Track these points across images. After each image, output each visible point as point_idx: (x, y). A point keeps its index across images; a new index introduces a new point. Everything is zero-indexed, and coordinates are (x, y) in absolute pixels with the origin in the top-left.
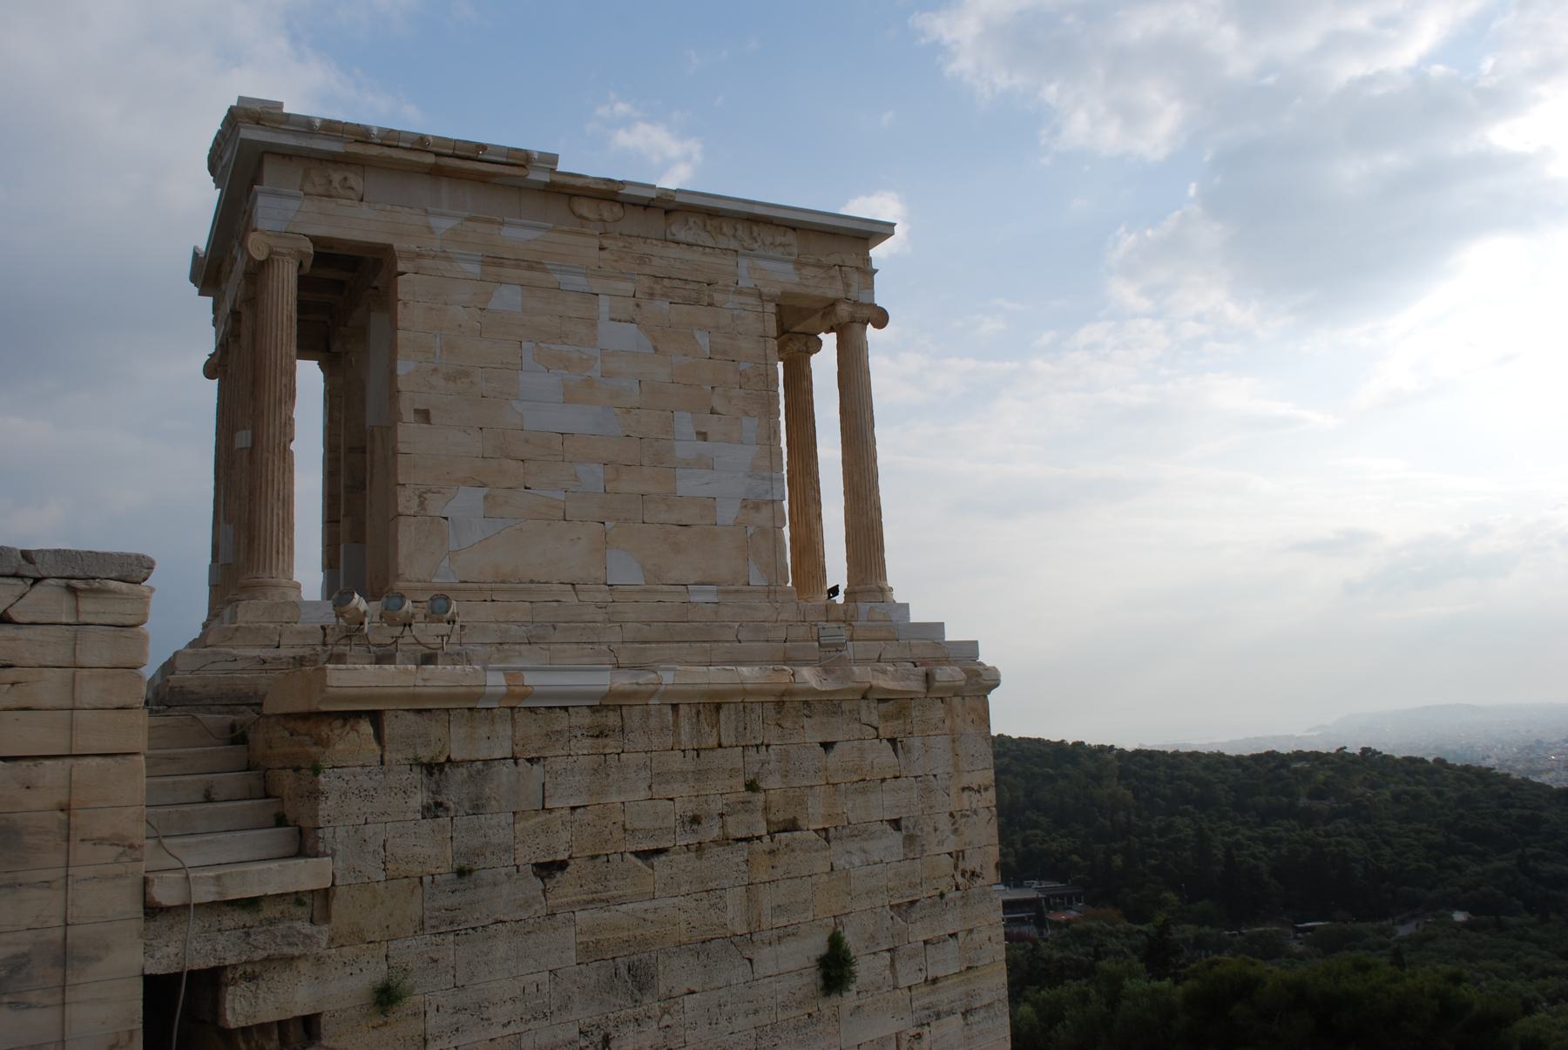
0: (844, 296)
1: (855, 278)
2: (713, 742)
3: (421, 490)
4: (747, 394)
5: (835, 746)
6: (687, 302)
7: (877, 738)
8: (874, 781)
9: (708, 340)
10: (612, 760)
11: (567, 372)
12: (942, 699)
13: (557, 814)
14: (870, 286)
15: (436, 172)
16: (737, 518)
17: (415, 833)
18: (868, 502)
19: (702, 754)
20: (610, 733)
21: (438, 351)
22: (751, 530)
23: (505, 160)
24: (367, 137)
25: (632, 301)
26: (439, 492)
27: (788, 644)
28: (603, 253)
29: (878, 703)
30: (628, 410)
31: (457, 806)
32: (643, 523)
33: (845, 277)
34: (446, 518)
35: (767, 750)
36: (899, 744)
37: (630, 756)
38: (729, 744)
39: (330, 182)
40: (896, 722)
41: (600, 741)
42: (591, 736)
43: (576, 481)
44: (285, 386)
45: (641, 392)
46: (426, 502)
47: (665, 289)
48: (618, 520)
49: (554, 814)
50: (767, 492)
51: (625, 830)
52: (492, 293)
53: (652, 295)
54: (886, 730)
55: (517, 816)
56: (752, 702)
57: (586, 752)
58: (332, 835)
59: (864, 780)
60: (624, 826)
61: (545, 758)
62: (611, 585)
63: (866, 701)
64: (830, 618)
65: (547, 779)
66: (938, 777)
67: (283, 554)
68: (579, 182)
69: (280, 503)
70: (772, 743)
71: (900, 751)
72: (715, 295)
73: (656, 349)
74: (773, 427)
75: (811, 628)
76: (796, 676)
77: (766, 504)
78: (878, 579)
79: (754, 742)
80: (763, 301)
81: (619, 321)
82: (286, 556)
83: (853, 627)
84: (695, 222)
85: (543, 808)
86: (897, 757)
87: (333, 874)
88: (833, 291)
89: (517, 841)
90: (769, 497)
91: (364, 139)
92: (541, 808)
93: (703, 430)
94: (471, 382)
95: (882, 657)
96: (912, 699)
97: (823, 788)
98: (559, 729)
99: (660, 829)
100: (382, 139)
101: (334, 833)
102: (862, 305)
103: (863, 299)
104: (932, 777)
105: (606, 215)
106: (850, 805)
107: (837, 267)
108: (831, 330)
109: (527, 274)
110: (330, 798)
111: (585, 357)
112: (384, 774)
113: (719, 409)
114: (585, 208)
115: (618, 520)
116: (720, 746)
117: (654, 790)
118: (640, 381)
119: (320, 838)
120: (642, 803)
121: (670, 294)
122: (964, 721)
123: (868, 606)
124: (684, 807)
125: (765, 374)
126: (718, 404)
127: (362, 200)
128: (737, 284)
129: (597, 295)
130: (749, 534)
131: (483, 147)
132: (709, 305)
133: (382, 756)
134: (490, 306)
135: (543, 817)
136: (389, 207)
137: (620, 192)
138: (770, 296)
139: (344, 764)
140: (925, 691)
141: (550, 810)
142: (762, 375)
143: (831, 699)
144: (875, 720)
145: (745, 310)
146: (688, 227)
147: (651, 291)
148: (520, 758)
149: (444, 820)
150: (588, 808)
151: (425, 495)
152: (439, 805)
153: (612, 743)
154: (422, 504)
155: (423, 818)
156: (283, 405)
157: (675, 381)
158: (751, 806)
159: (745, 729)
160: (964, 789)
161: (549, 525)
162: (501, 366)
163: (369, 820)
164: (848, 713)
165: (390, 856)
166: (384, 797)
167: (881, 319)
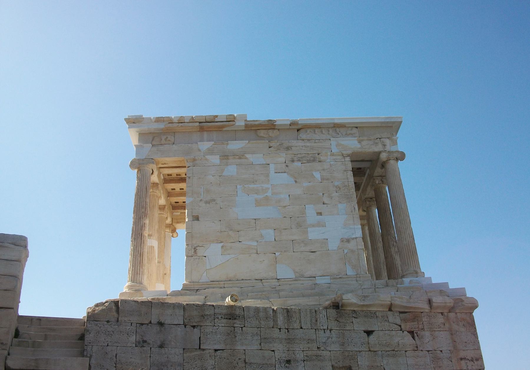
0: (383, 150)
1: (387, 142)
2: (296, 325)
3: (196, 246)
4: (340, 194)
5: (374, 333)
6: (309, 161)
7: (401, 330)
8: (400, 351)
9: (320, 175)
10: (238, 330)
11: (257, 195)
13: (207, 352)
14: (395, 143)
15: (202, 129)
16: (338, 247)
17: (132, 352)
19: (291, 331)
20: (237, 318)
21: (202, 193)
22: (346, 251)
23: (225, 120)
24: (172, 121)
25: (284, 165)
26: (202, 246)
28: (270, 148)
30: (285, 207)
31: (154, 343)
32: (294, 252)
34: (205, 257)
35: (330, 332)
36: (415, 334)
37: (249, 329)
38: (307, 328)
39: (162, 139)
41: (231, 320)
42: (226, 318)
43: (262, 237)
44: (143, 212)
45: (290, 199)
46: (197, 251)
47: (299, 158)
48: (282, 251)
49: (205, 352)
50: (353, 234)
51: (246, 363)
52: (224, 169)
53: (293, 161)
54: (409, 326)
55: (185, 351)
57: (223, 325)
58: (91, 349)
59: (394, 350)
60: (245, 361)
61: (201, 326)
62: (279, 279)
63: (392, 312)
65: (202, 336)
66: (443, 352)
67: (139, 274)
68: (257, 123)
69: (139, 255)
70: (333, 328)
71: (416, 338)
72: (321, 157)
73: (296, 182)
74: (354, 207)
78: (414, 268)
79: (322, 328)
80: (344, 157)
81: (279, 173)
82: (141, 275)
84: (310, 131)
85: (200, 348)
86: (414, 340)
87: (89, 364)
88: (376, 149)
89: (185, 361)
90: (354, 236)
91: (172, 122)
92: (198, 348)
93: (320, 211)
94: (216, 203)
96: (422, 313)
97: (367, 353)
98: (209, 314)
99: (267, 364)
100: (178, 121)
101: (92, 348)
103: (393, 149)
104: (439, 352)
105: (271, 134)
106: (385, 362)
109: (239, 160)
110: (91, 333)
111: (264, 188)
112: (118, 325)
113: (326, 202)
114: (262, 133)
115: (282, 251)
116: (301, 328)
117: (262, 346)
118: (289, 195)
119: (85, 349)
120: (256, 351)
121: (301, 160)
124: (280, 355)
125: (348, 185)
126: (326, 200)
127: (174, 144)
129: (269, 164)
130: (345, 253)
131: (217, 116)
132: (320, 162)
133: (118, 318)
134: (224, 174)
135: (198, 352)
136: (183, 145)
137: (274, 124)
138: (347, 154)
139: (99, 320)
141: (204, 350)
142: (346, 186)
143: (370, 310)
144: (398, 321)
146: (307, 133)
147: (292, 160)
148: (187, 325)
149: (147, 348)
150: (224, 350)
151: (196, 248)
152: (145, 342)
153: (238, 322)
154: (195, 252)
155: (136, 346)
156: (142, 219)
157: (305, 193)
158: (321, 358)
159: (316, 321)
160: (461, 359)
161: (250, 256)
162: (228, 196)
163: (109, 344)
164: (380, 317)
165: (119, 361)
166: (117, 335)
167: (401, 156)
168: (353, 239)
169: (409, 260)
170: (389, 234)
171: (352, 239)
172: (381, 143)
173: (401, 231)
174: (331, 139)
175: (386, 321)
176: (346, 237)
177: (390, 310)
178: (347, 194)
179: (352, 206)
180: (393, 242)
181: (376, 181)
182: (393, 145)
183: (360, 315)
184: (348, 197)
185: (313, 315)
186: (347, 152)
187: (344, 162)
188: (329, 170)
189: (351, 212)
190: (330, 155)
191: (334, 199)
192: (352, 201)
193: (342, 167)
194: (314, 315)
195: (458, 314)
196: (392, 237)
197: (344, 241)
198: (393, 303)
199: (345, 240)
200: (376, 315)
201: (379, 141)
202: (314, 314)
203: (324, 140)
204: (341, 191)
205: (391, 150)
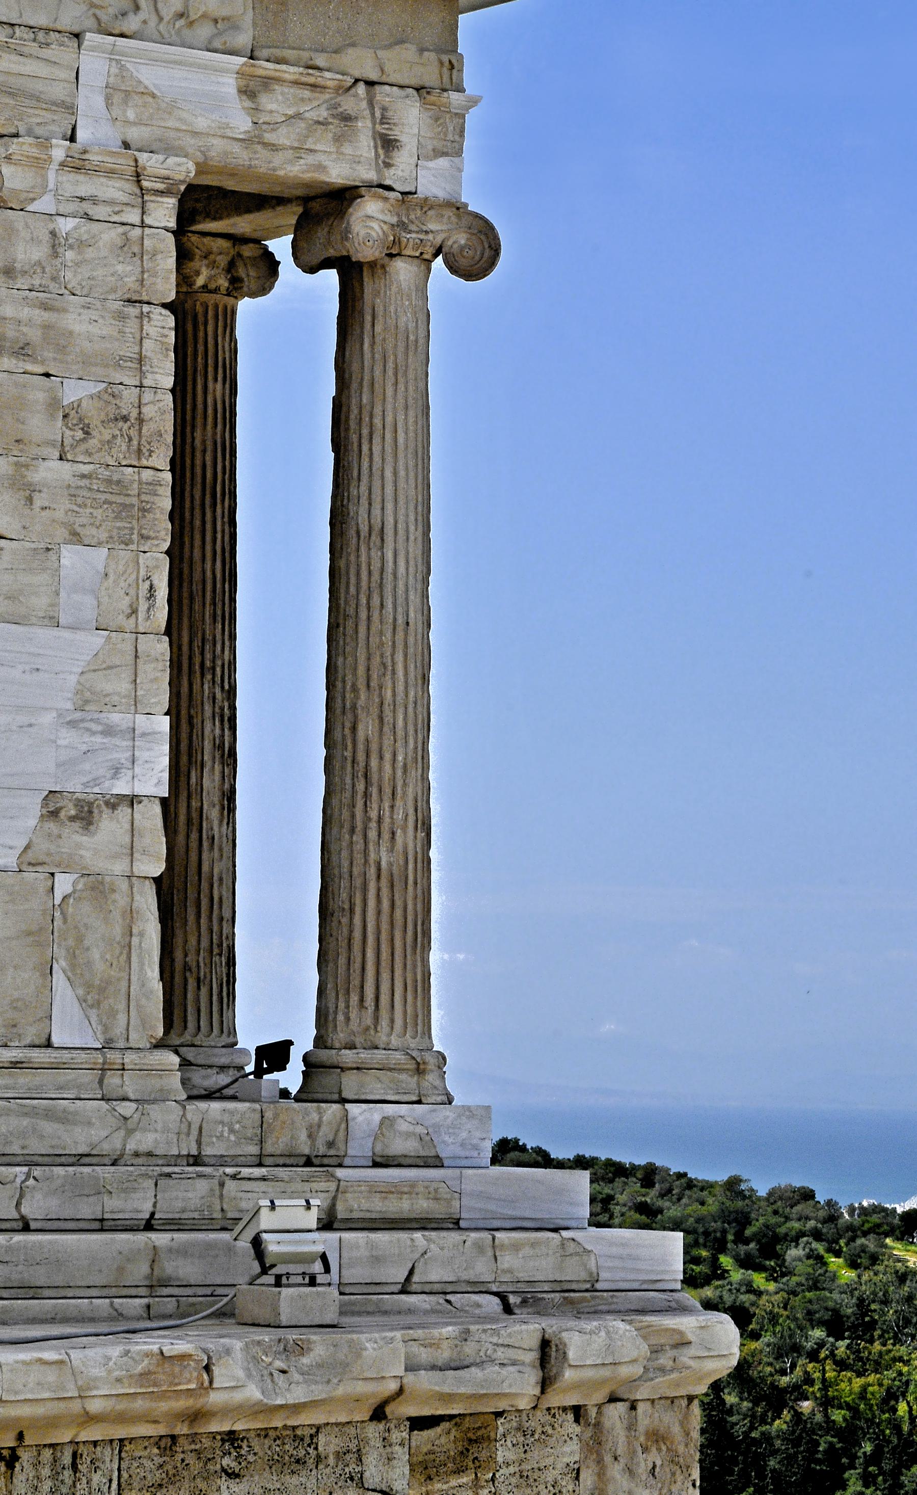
0: (371, 175)
4: (83, 476)
12: (578, 1412)
16: (27, 847)
18: (399, 803)
22: (64, 884)
27: (160, 1239)
29: (412, 1429)
33: (384, 120)
40: (454, 1482)
50: (116, 771)
56: (95, 1443)
63: (381, 1426)
64: (269, 1148)
75: (222, 1185)
76: (216, 1370)
77: (113, 806)
83: (339, 1181)
90: (121, 787)
95: (416, 1278)
96: (499, 1414)
102: (427, 205)
107: (361, 89)
108: (327, 264)
122: (630, 1471)
123: (377, 1113)
125: (134, 414)
128: (72, 139)
130: (57, 901)
140: (537, 1391)
142: (125, 419)
145: (88, 217)
164: (331, 1460)
168: (114, 803)
169: (385, 976)
170: (208, 664)
171: (107, 803)
172: (374, 124)
173: (375, 777)
174: (90, 38)
175: (352, 1479)
176: (74, 785)
177: (378, 1414)
178: (119, 482)
179: (142, 573)
180: (222, 721)
181: (198, 273)
182: (439, 153)
183: (251, 1458)
184: (124, 506)
185: (62, 1482)
186: (172, 160)
187: (137, 232)
188: (37, 282)
189: (129, 616)
190: (62, 165)
191: (44, 508)
192: (142, 536)
193: (120, 268)
194: (66, 1481)
195: (641, 1407)
196: (218, 690)
197: (62, 814)
198: (406, 1388)
199: (71, 806)
200: (316, 1449)
201: (364, 104)
202: (67, 1474)
203: (41, 35)
204: (88, 453)
205: (420, 195)
